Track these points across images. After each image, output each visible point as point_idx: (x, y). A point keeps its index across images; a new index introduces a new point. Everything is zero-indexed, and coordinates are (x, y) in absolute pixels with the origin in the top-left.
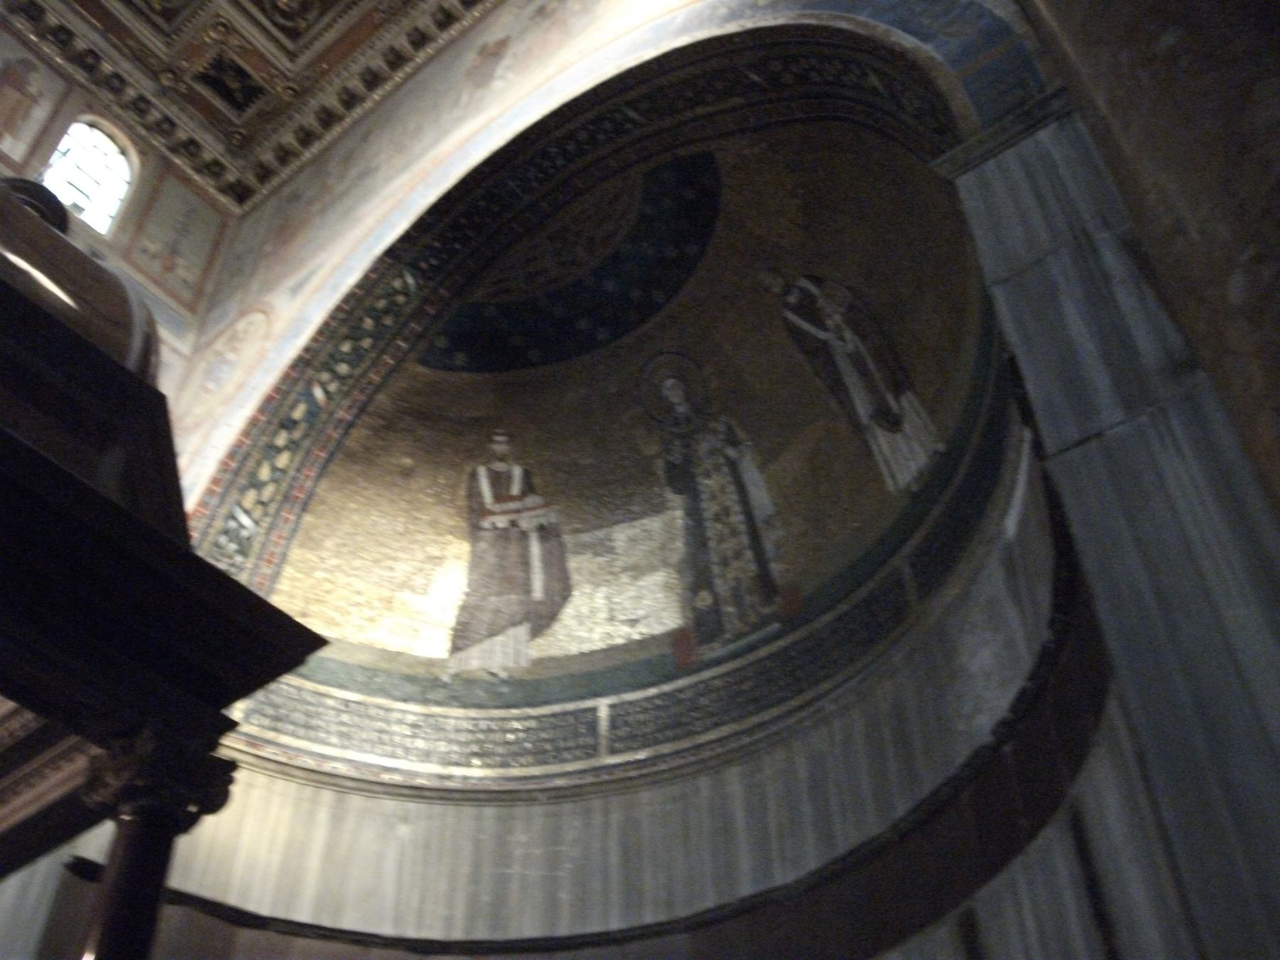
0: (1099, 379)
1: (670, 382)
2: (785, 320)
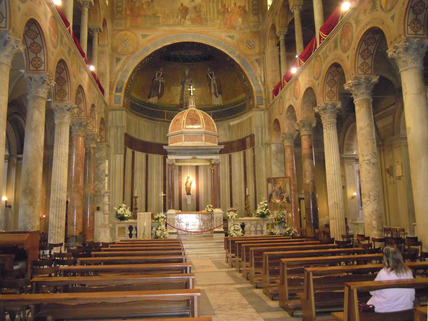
0: (260, 142)
1: (187, 71)
2: (207, 74)
